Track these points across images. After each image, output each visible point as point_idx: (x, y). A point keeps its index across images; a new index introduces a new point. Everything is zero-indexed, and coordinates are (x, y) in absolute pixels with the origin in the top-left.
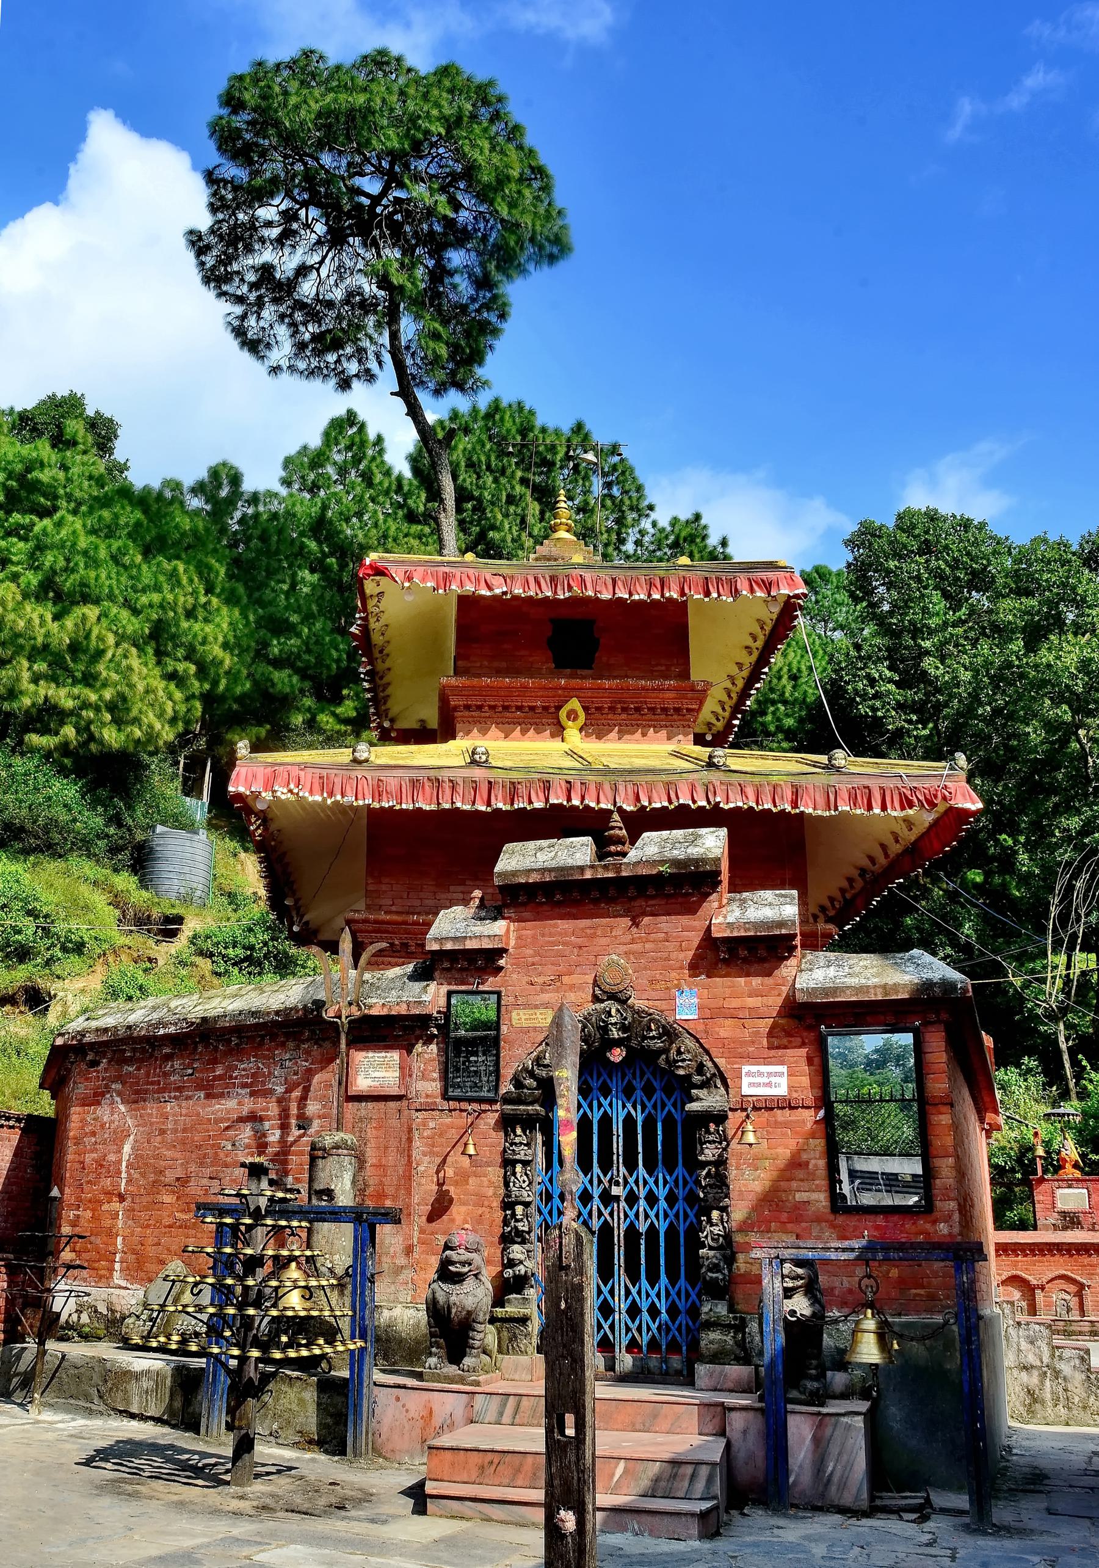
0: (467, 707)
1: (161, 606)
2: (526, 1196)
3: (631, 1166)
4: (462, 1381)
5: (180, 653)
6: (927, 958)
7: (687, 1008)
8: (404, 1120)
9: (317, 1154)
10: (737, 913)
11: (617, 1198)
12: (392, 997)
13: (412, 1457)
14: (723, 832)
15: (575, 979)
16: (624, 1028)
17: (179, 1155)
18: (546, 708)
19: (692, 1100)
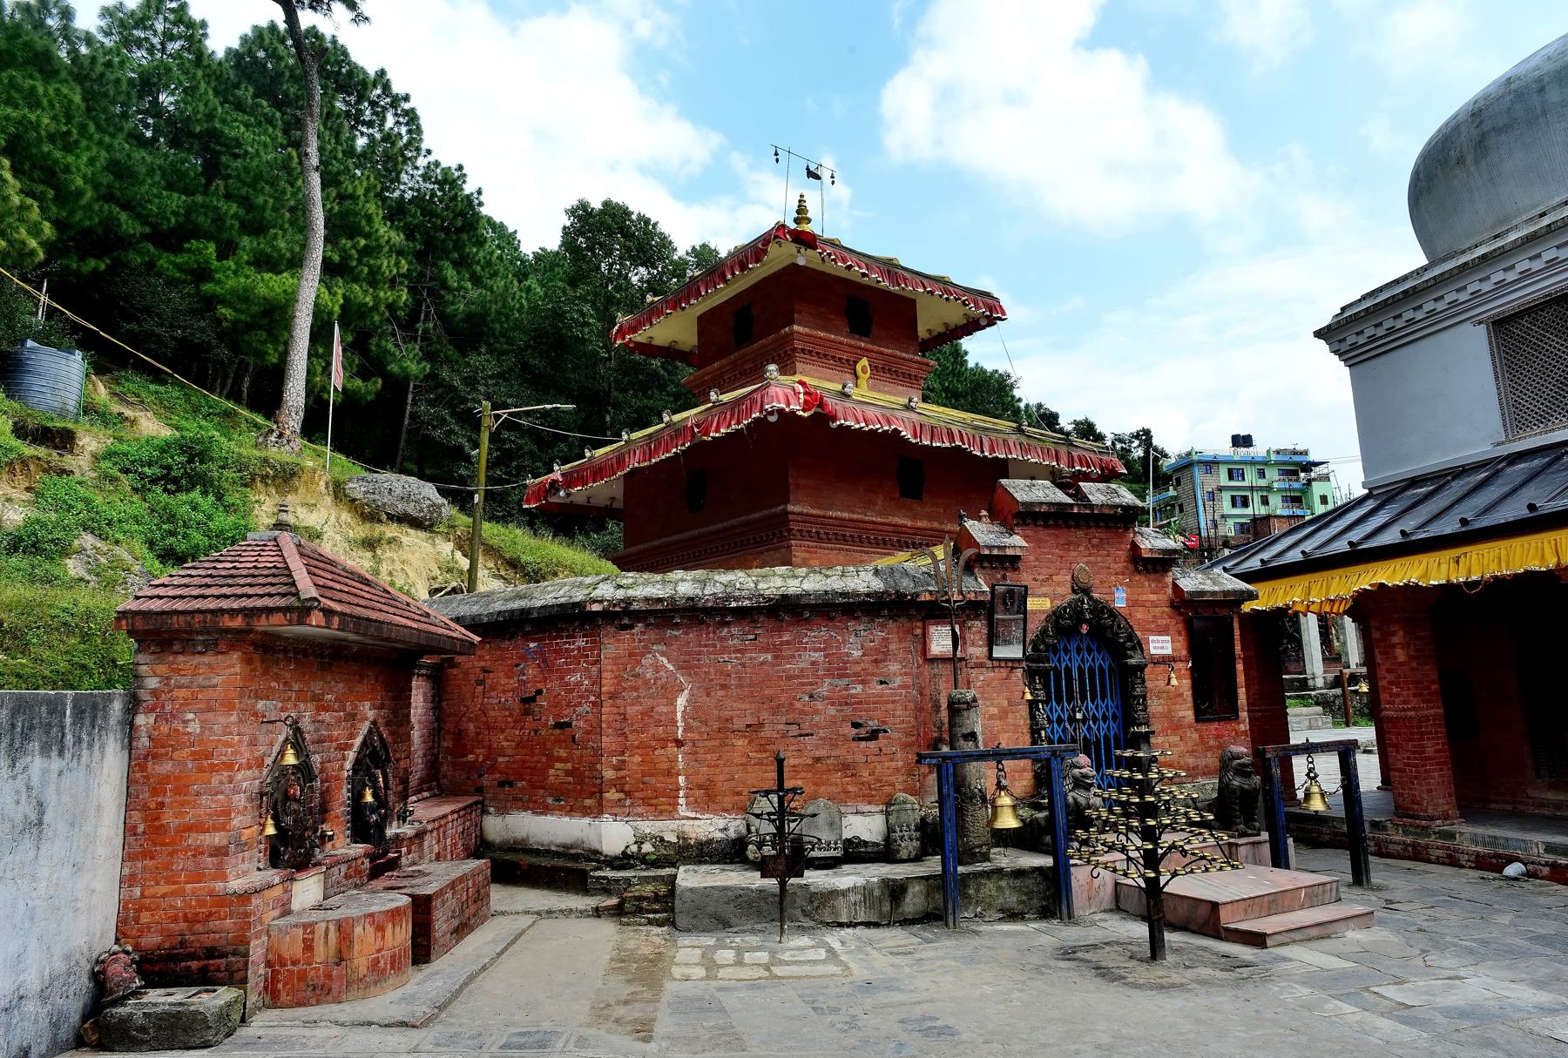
3: (1083, 698)
7: (1120, 601)
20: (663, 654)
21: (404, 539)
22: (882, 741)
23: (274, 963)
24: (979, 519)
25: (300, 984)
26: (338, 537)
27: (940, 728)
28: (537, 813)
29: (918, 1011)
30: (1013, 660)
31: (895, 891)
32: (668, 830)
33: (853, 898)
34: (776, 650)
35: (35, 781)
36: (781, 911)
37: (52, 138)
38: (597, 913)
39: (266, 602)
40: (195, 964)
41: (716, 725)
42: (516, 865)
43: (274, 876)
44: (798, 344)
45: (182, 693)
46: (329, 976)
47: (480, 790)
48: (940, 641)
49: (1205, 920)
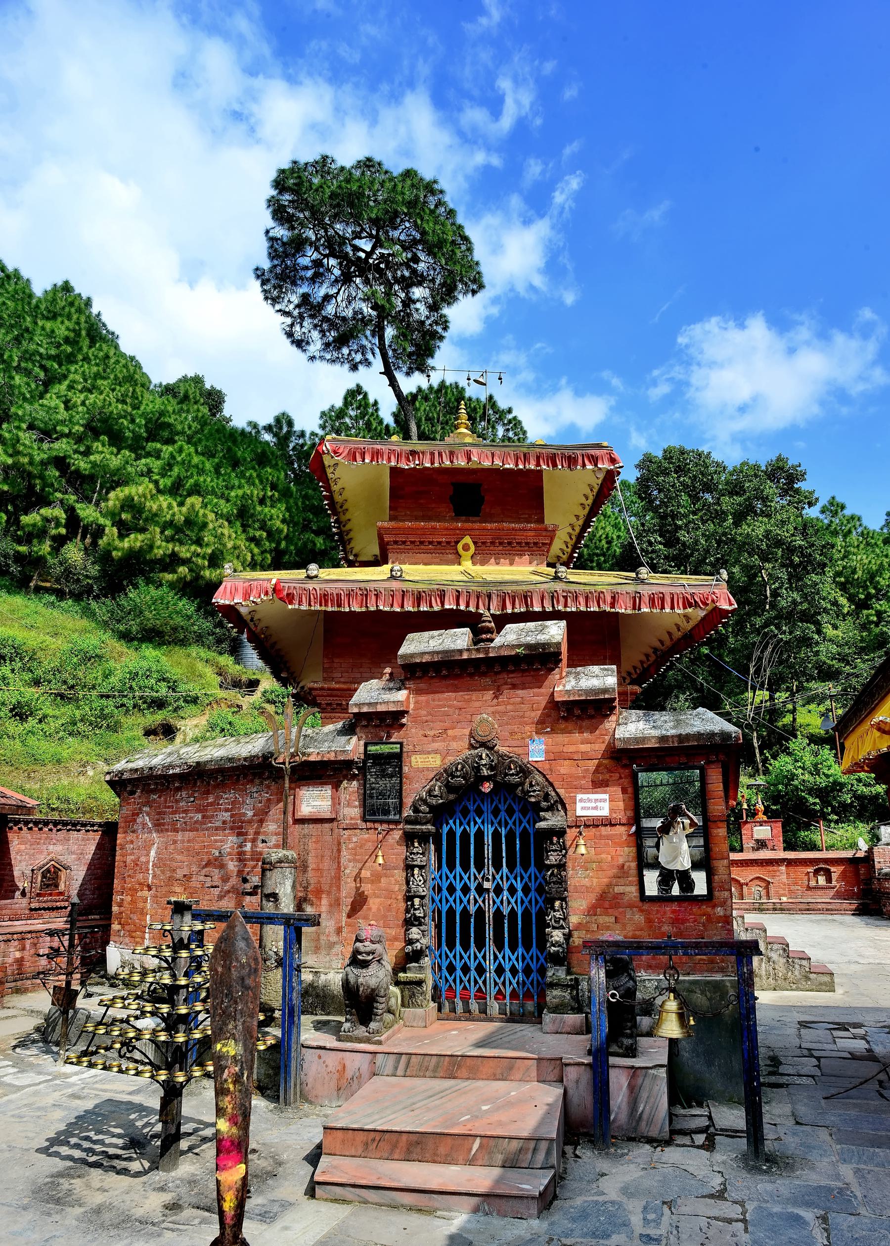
0: (396, 542)
1: (243, 497)
2: (422, 891)
3: (498, 866)
4: (368, 1041)
5: (257, 525)
6: (710, 714)
7: (537, 752)
8: (335, 836)
9: (267, 867)
10: (573, 683)
11: (488, 890)
12: (325, 747)
13: (330, 1101)
14: (563, 624)
15: (457, 732)
16: (491, 768)
17: (185, 859)
18: (448, 543)
19: (541, 820)
20: (148, 814)
27: (305, 888)
37: (262, 501)
41: (168, 874)
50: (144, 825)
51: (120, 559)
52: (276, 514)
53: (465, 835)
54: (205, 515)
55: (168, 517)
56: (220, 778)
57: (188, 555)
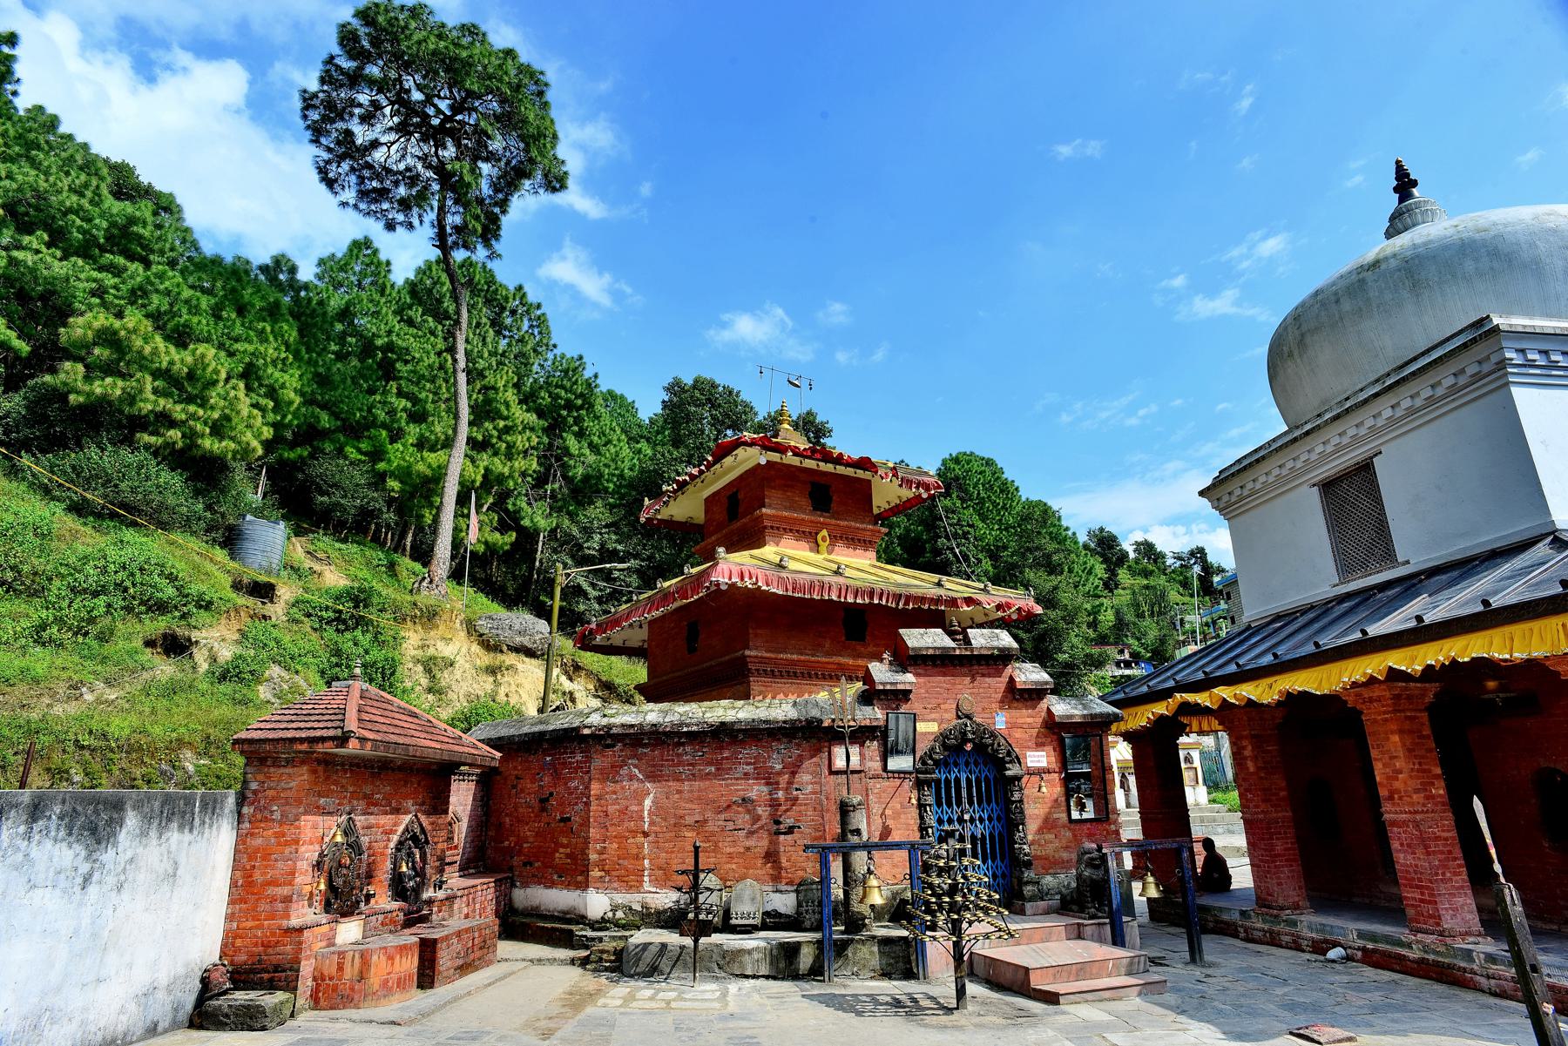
5: (262, 391)
7: (1000, 722)
21: (520, 666)
22: (796, 836)
23: (318, 978)
24: (881, 660)
25: (329, 995)
26: (467, 666)
28: (547, 887)
29: (749, 1032)
30: (905, 773)
31: (791, 951)
32: (634, 900)
33: (756, 956)
34: (718, 764)
35: (173, 848)
36: (694, 963)
38: (572, 962)
39: (325, 733)
40: (266, 976)
42: (527, 925)
43: (324, 918)
44: (767, 523)
45: (270, 793)
46: (352, 989)
47: (511, 869)
48: (839, 754)
49: (1012, 982)
50: (631, 778)
51: (80, 406)
52: (291, 382)
53: (947, 781)
54: (216, 372)
55: (164, 365)
56: (741, 737)
57: (184, 417)
